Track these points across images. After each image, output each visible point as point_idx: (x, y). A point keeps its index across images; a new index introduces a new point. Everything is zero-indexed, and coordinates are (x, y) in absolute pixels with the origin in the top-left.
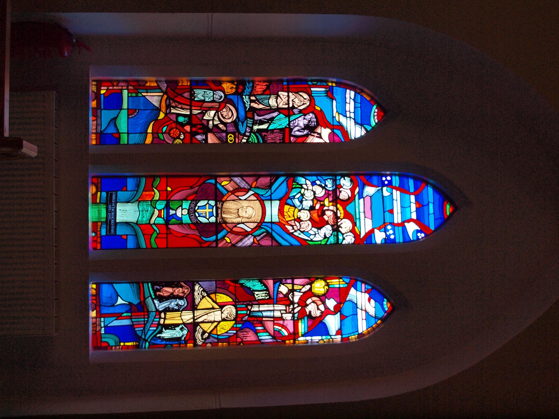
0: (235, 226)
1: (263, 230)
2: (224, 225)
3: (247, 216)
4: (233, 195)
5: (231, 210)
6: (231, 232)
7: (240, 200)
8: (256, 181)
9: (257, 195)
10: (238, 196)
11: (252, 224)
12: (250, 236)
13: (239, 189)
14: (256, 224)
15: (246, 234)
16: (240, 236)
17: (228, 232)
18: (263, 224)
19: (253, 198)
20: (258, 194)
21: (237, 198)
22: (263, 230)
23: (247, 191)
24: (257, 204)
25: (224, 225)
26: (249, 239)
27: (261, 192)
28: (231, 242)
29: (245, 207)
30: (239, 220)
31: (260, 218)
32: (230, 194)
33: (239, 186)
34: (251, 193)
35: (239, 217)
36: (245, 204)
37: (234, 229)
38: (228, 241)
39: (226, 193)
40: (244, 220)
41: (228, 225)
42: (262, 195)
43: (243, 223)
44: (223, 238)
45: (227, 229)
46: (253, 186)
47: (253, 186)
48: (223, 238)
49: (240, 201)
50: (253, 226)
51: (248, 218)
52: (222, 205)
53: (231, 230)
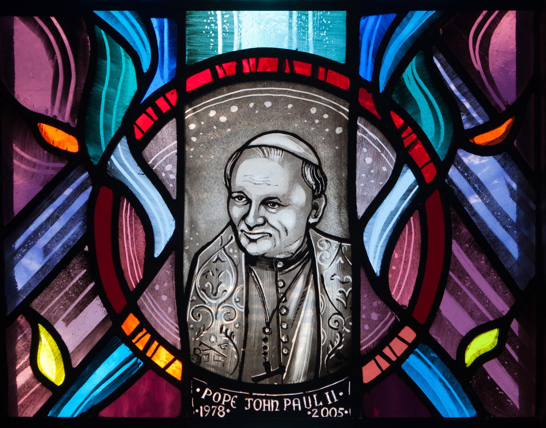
0: (381, 285)
1: (411, 77)
2: (370, 372)
3: (300, 196)
4: (146, 302)
5: (258, 317)
6: (420, 315)
7: (176, 242)
8: (30, 122)
9: (143, 122)
10: (152, 265)
11: (365, 159)
12: (453, 173)
13: (97, 260)
14: (367, 133)
15: (439, 211)
16: (456, 248)
17: (424, 342)
18: (365, 71)
19: (163, 149)
20: (136, 107)
21: (166, 272)
22: (411, 77)
23: (112, 194)
24: (215, 116)
25: (370, 372)
26: (480, 188)
27: (120, 87)
28: (500, 323)
29: (237, 211)
30: (329, 259)
31: (320, 102)
32: (131, 323)
33: (73, 252)
34: (123, 162)
35: (306, 256)
36: (210, 210)
37: (402, 291)
38: (486, 341)
39: (122, 352)
40: (333, 221)
41: (367, 341)
42: (144, 79)
43: (356, 227)
44: (469, 379)
45: (398, 347)
46: (71, 145)
47: (71, 145)
48: (469, 379)
49: (189, 249)
50: (374, 156)
51: (317, 192)
52: (217, 381)
53: (404, 316)
